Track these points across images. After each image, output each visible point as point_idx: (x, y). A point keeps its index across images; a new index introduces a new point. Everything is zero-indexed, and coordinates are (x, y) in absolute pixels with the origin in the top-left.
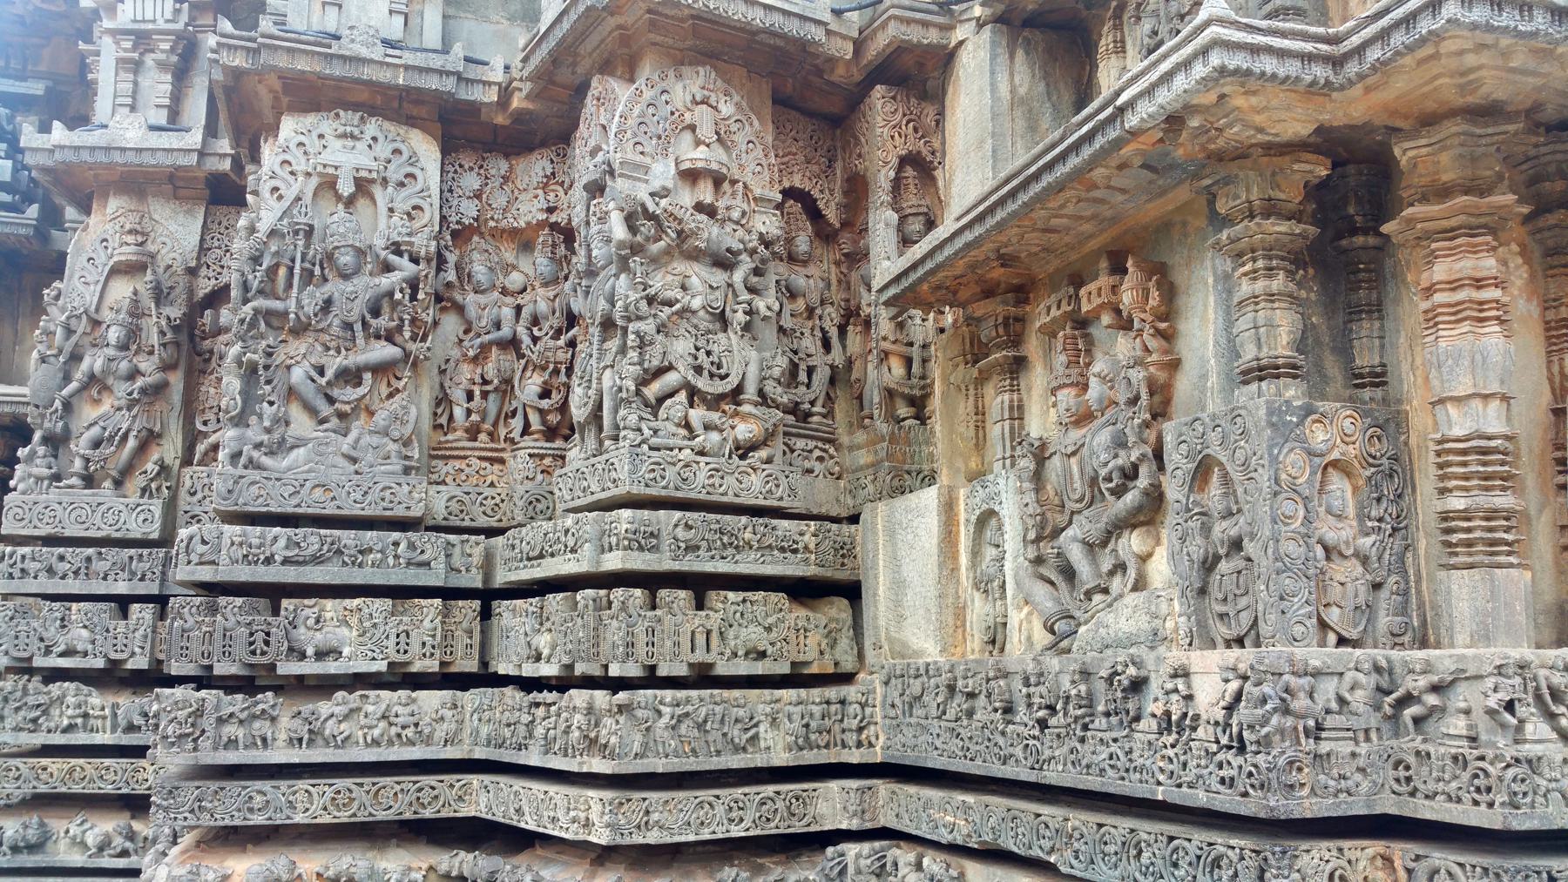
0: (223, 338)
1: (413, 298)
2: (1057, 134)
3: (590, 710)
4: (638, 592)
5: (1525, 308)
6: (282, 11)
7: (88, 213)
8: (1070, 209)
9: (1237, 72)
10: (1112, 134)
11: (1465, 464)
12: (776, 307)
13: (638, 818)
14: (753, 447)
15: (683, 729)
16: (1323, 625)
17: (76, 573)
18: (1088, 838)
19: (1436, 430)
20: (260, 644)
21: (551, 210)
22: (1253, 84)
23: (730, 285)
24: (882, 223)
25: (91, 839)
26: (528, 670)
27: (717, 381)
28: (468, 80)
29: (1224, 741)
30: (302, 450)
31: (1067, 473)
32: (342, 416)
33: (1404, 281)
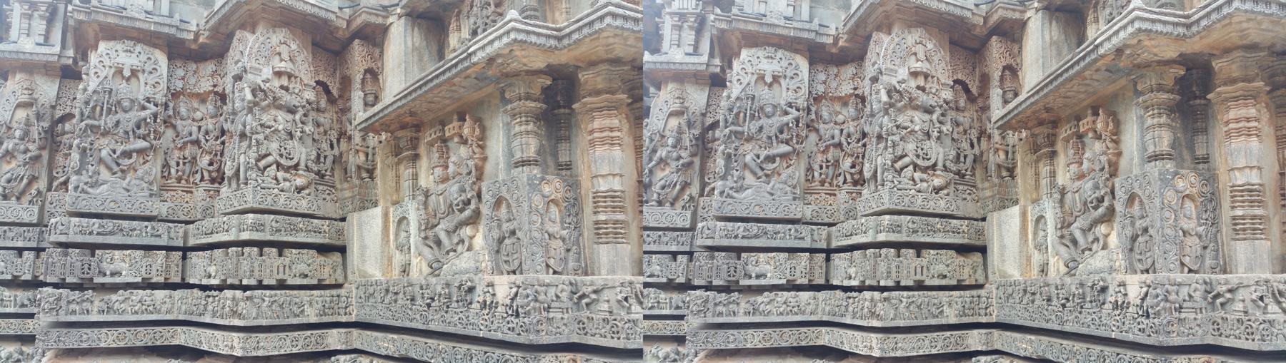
0: (716, 143)
1: (797, 126)
2: (1070, 57)
3: (872, 300)
4: (892, 250)
5: (1268, 130)
6: (742, 4)
7: (660, 90)
8: (1075, 88)
9: (1146, 30)
10: (1093, 56)
11: (1242, 196)
12: (951, 130)
13: (892, 346)
14: (941, 189)
15: (911, 308)
16: (1183, 264)
17: (655, 242)
18: (1083, 354)
19: (1230, 182)
20: (732, 272)
21: (855, 89)
22: (1153, 36)
23: (931, 121)
24: (995, 94)
25: (661, 354)
26: (846, 283)
27: (926, 161)
28: (820, 34)
29: (1140, 313)
30: (750, 190)
31: (1074, 200)
32: (767, 176)
33: (1217, 119)
